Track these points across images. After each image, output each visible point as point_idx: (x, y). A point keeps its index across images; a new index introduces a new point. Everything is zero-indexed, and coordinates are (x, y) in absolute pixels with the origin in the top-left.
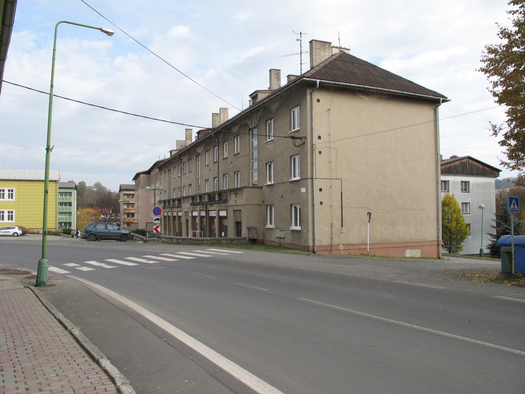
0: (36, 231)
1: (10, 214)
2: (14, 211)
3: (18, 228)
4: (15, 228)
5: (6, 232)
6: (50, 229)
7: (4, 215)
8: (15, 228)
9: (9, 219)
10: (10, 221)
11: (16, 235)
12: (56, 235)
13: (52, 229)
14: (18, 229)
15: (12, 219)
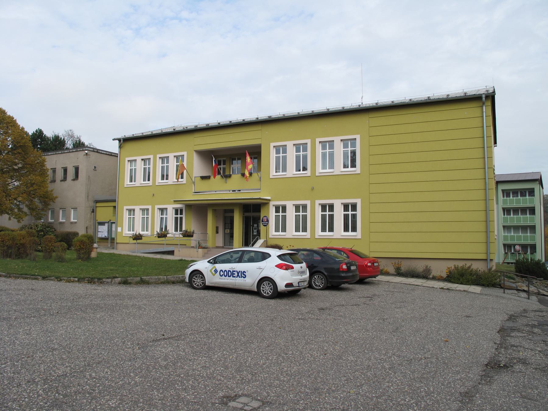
0: (420, 267)
1: (350, 213)
2: (359, 202)
3: (279, 257)
4: (269, 256)
5: (232, 274)
6: (468, 264)
7: (333, 215)
8: (269, 256)
9: (346, 229)
10: (350, 233)
11: (267, 289)
12: (488, 286)
13: (473, 263)
14: (280, 262)
15: (354, 229)
